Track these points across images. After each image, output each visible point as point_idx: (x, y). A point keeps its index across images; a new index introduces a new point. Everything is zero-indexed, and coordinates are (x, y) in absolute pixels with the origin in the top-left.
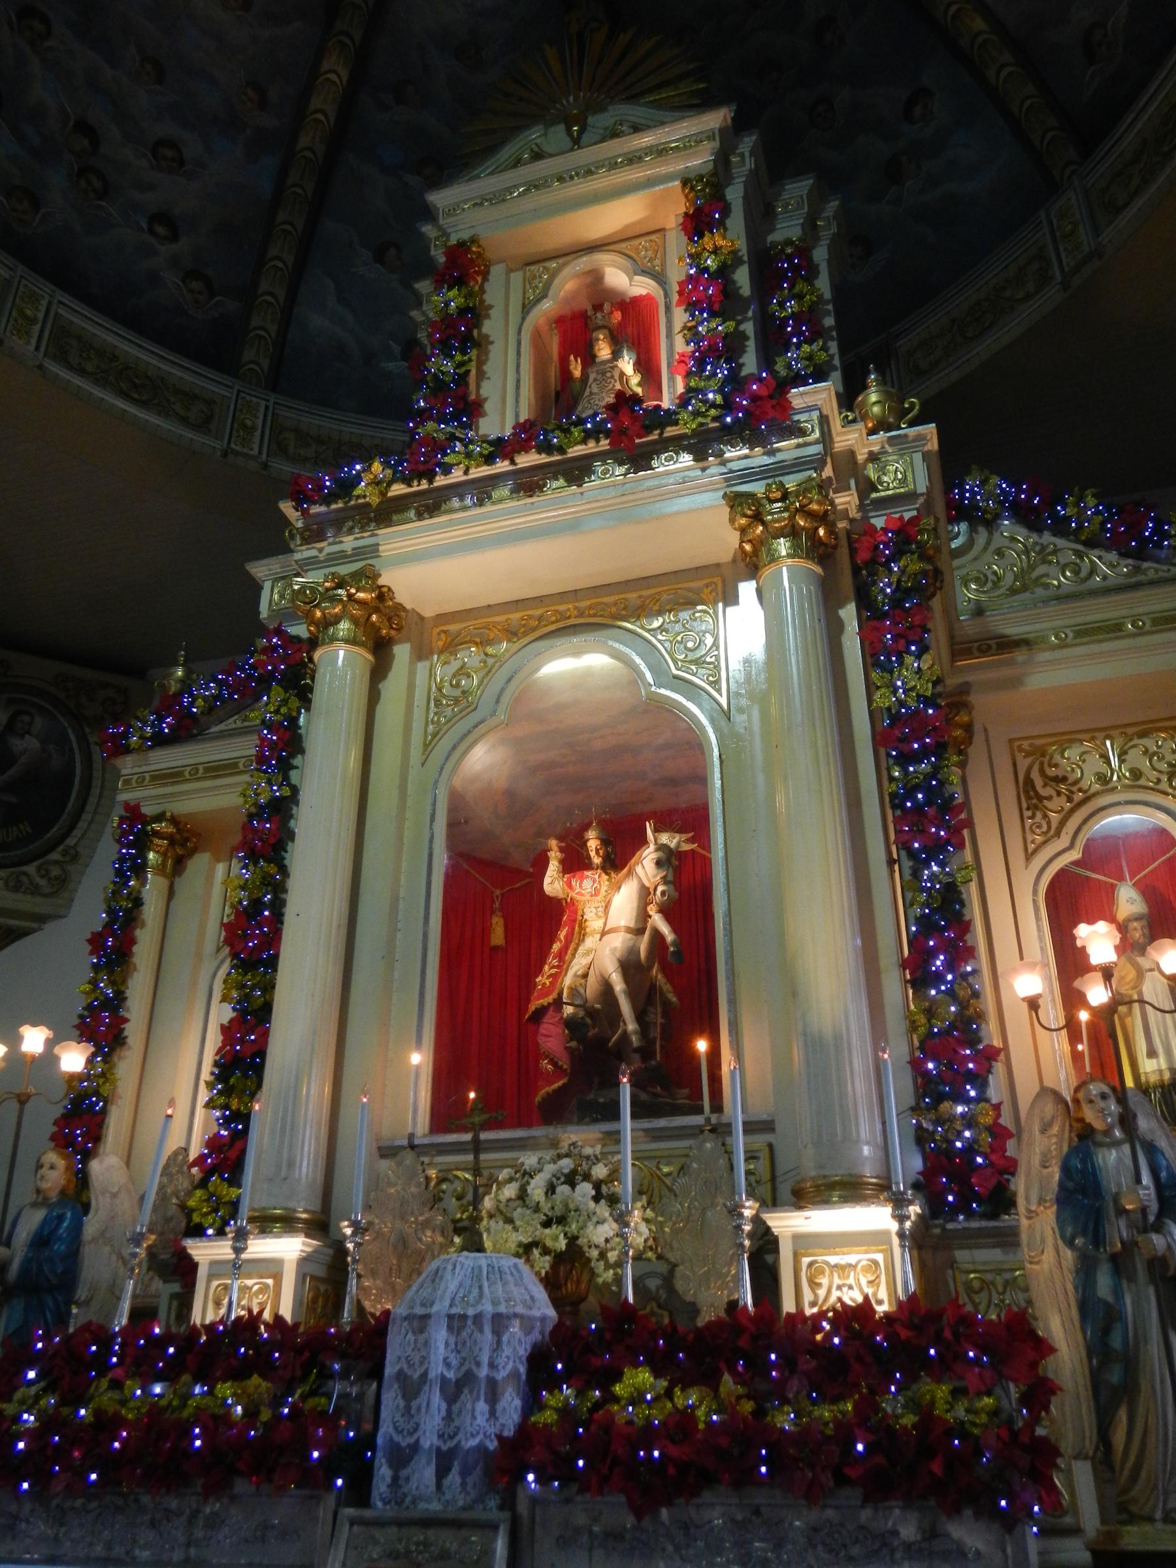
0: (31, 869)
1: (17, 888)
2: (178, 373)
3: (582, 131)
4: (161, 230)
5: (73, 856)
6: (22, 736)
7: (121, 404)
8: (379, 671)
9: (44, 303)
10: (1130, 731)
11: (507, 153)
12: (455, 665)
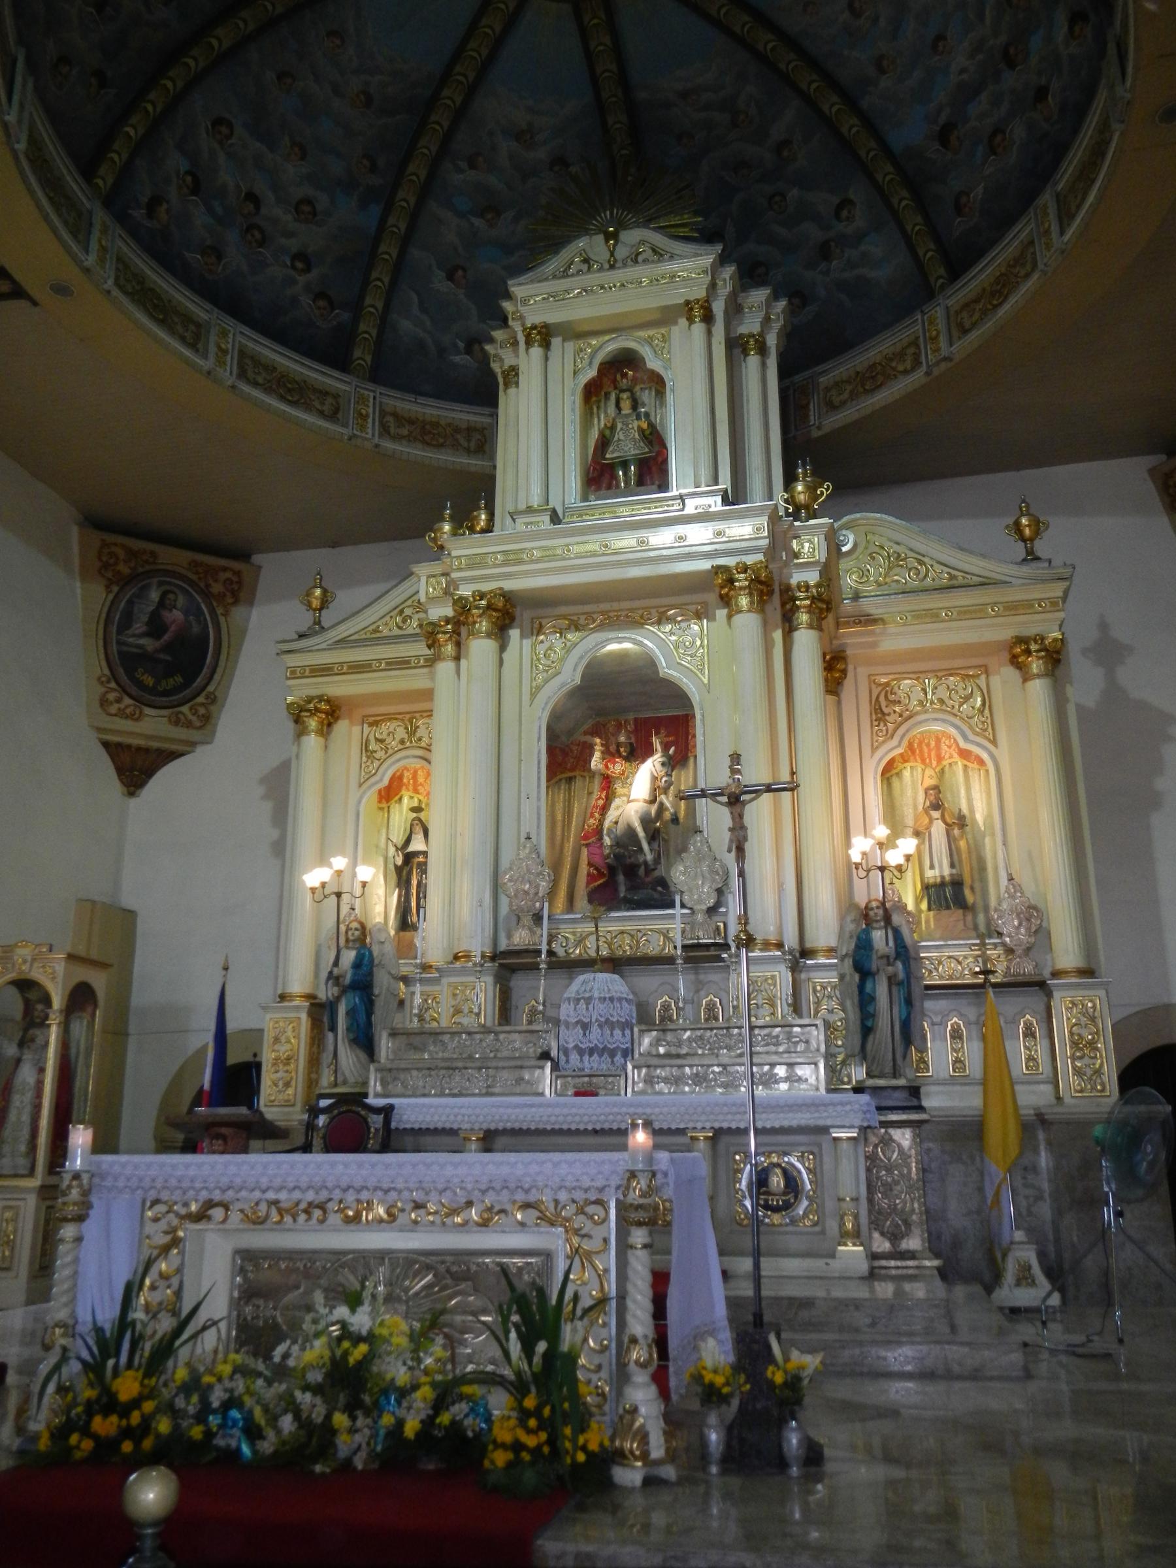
0: (185, 709)
1: (177, 723)
2: (314, 375)
3: (615, 245)
4: (299, 265)
5: (213, 699)
6: (171, 610)
7: (283, 407)
8: (503, 648)
9: (231, 336)
10: (940, 674)
11: (566, 254)
12: (547, 645)
